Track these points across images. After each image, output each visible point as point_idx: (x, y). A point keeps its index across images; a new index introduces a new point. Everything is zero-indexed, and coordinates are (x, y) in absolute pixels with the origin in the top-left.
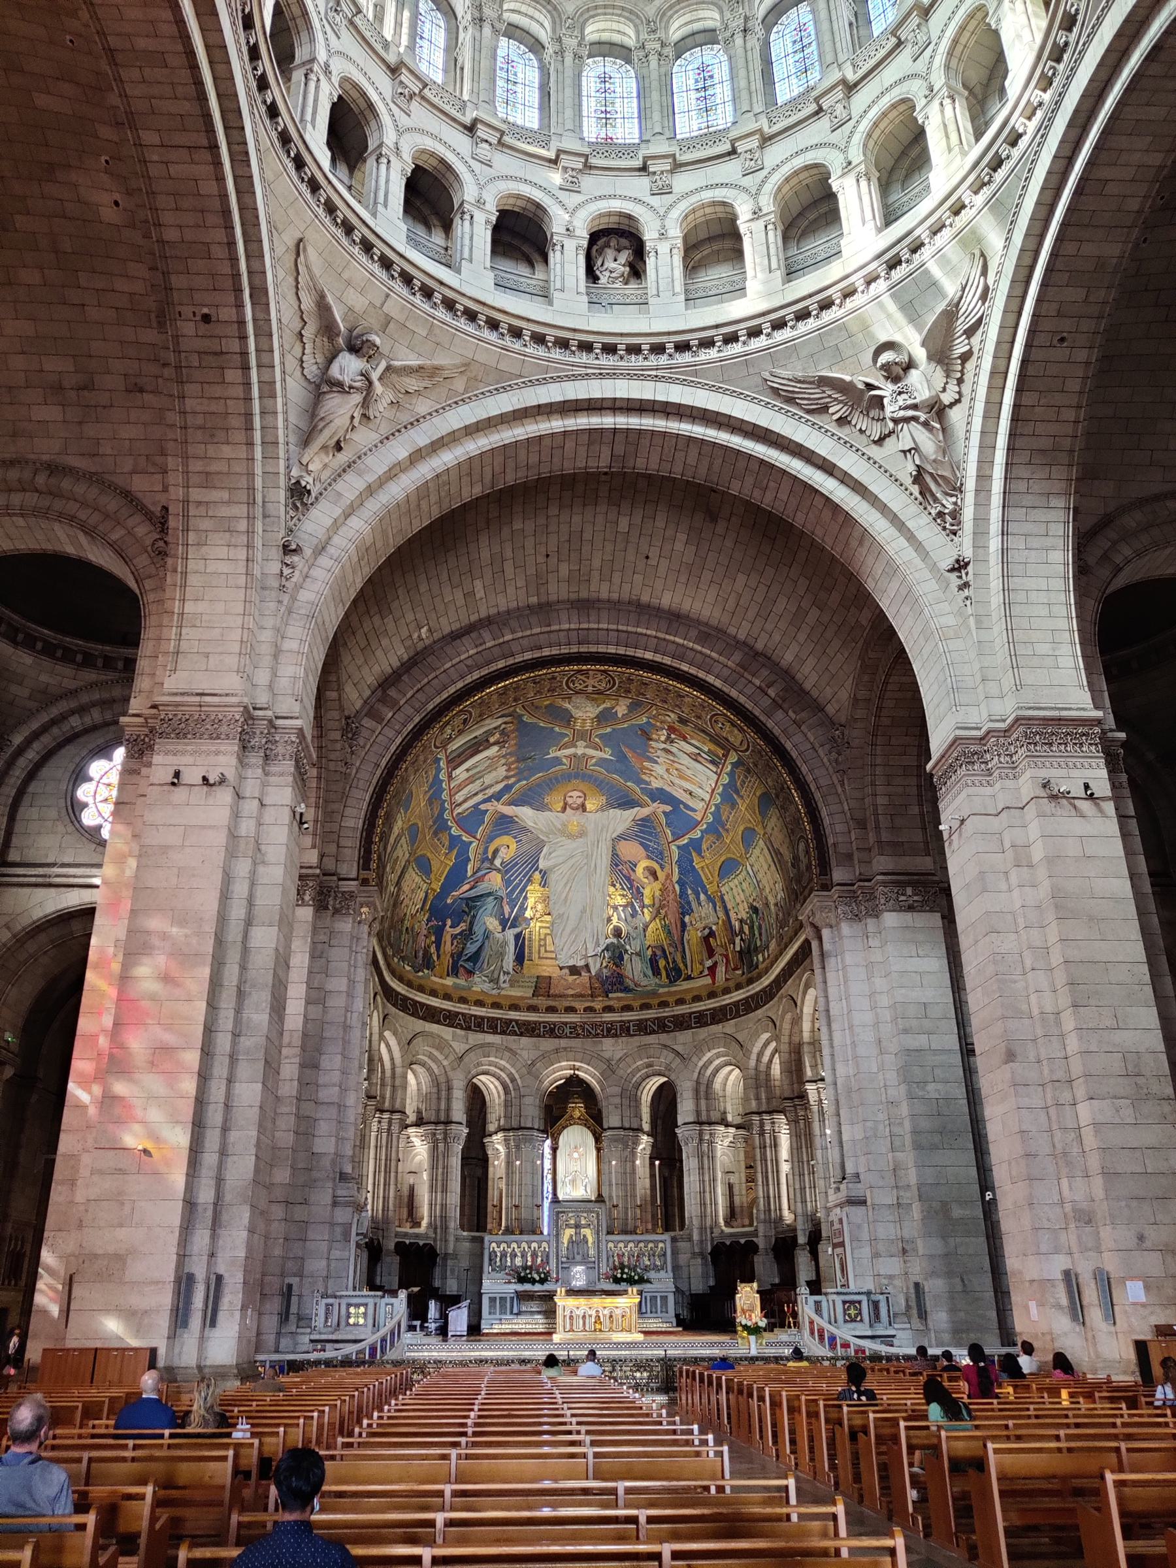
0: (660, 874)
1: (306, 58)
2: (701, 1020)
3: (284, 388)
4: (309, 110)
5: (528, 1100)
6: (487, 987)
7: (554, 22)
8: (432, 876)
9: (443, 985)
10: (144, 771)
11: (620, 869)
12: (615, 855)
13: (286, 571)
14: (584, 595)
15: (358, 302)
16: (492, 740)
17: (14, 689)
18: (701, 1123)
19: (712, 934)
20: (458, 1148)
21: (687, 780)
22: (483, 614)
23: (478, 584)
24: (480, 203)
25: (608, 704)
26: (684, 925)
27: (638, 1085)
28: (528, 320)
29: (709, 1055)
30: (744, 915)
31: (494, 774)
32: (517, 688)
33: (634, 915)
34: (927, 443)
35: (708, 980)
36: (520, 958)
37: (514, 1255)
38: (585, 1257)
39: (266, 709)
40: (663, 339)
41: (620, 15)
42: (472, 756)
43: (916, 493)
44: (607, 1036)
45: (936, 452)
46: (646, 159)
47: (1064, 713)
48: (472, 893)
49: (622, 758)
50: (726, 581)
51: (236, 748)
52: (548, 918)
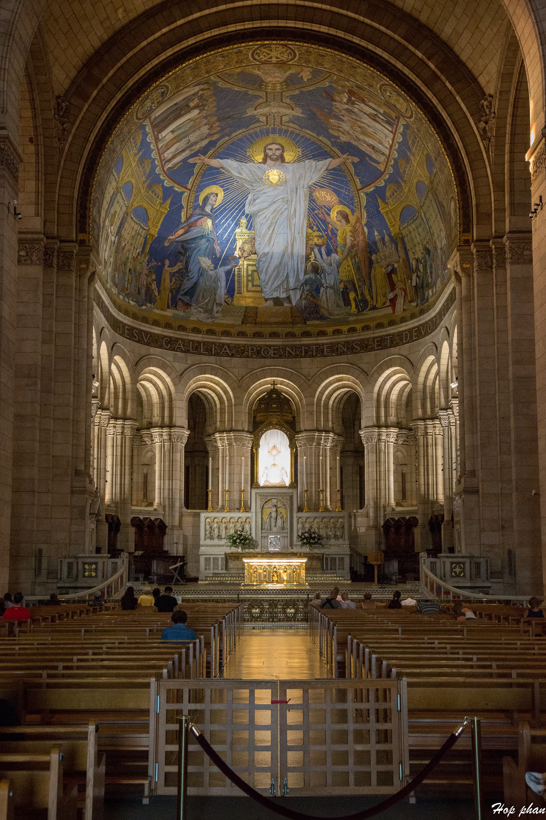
8: (150, 223)
9: (164, 316)
12: (312, 200)
16: (192, 105)
18: (379, 426)
19: (394, 271)
20: (181, 446)
21: (369, 137)
25: (293, 71)
26: (371, 263)
30: (419, 255)
31: (198, 133)
33: (329, 254)
35: (390, 310)
36: (231, 291)
44: (305, 357)
52: (254, 257)
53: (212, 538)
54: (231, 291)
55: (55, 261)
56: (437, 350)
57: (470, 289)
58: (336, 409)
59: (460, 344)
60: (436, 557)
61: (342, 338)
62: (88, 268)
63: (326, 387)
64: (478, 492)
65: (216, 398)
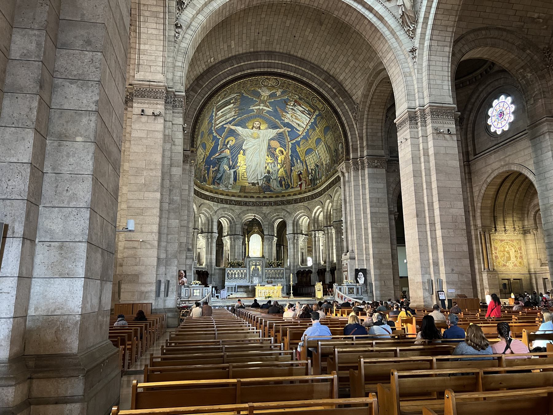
2: (296, 201)
5: (238, 226)
6: (224, 189)
11: (271, 151)
12: (269, 145)
13: (177, 35)
14: (270, 49)
16: (232, 102)
18: (294, 234)
19: (301, 173)
20: (215, 241)
22: (233, 54)
23: (233, 42)
26: (291, 170)
27: (274, 222)
29: (298, 212)
31: (230, 114)
32: (244, 83)
35: (299, 188)
36: (235, 179)
37: (235, 274)
38: (258, 274)
39: (172, 88)
43: (401, 22)
45: (410, 7)
47: (444, 105)
48: (219, 157)
49: (276, 111)
50: (322, 47)
51: (164, 103)
56: (322, 204)
60: (341, 285)
61: (279, 199)
64: (355, 259)
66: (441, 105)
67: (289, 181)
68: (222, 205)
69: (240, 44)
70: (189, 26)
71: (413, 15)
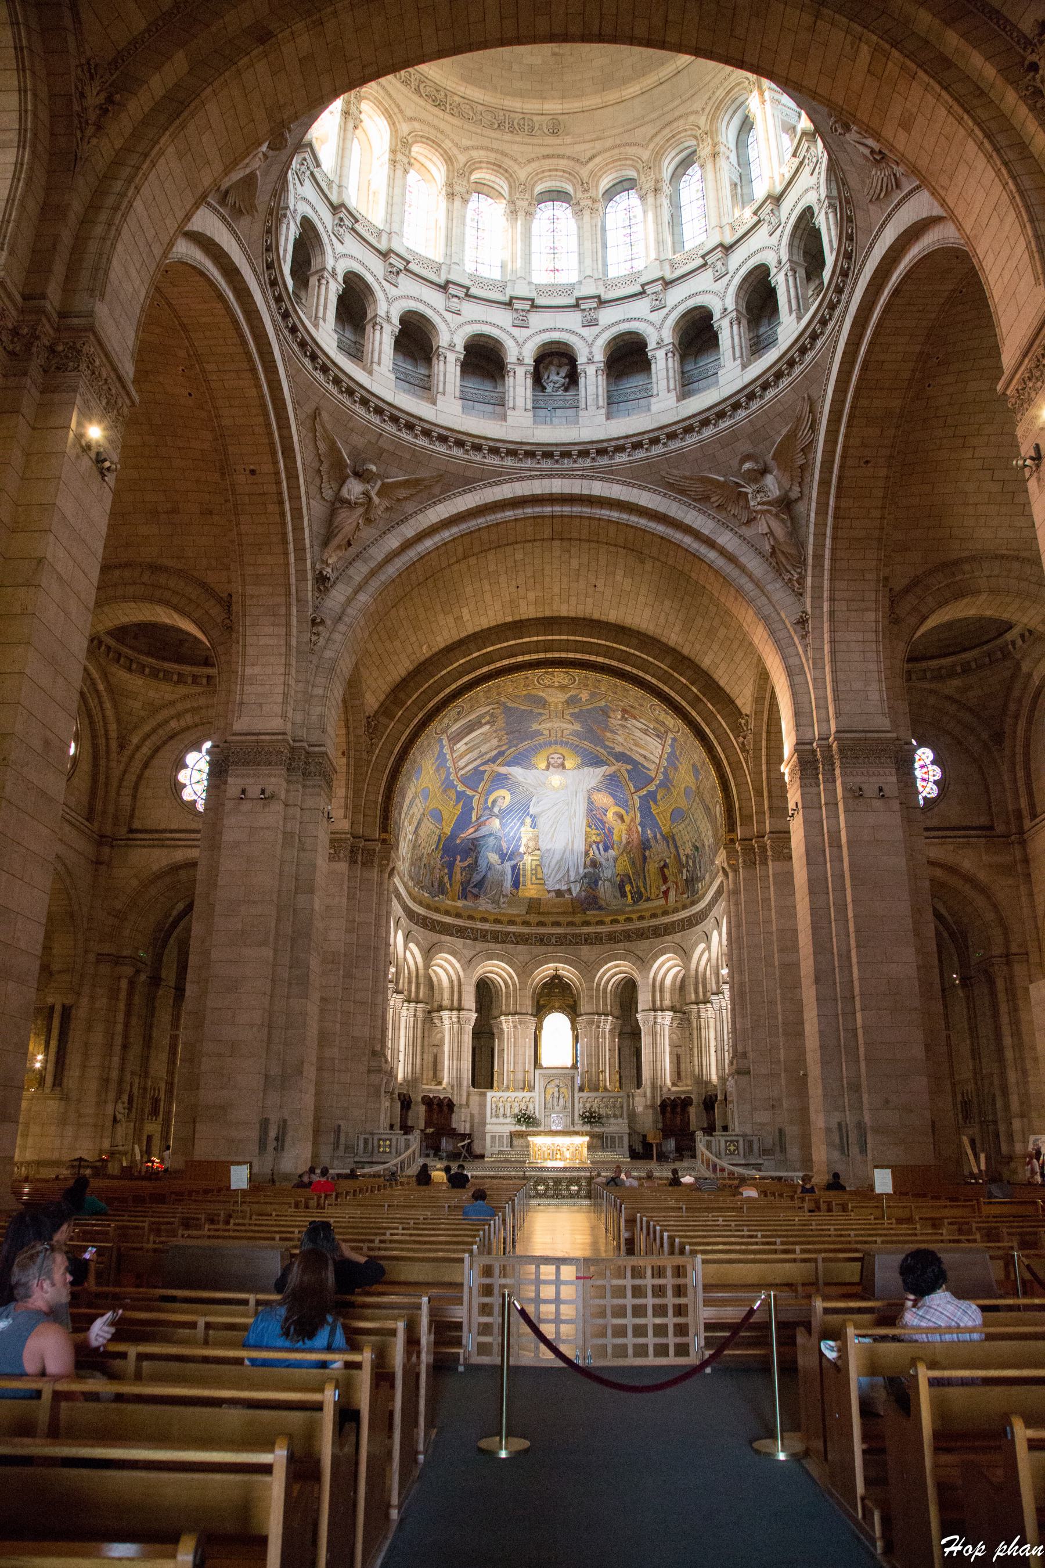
0: (625, 817)
1: (319, 267)
3: (309, 509)
4: (321, 308)
6: (490, 907)
7: (510, 187)
8: (444, 823)
9: (455, 907)
10: (223, 786)
12: (590, 802)
13: (314, 638)
14: (548, 613)
15: (359, 441)
16: (483, 721)
17: (131, 702)
18: (655, 1010)
19: (665, 866)
20: (469, 1028)
22: (470, 631)
23: (465, 611)
24: (452, 347)
25: (573, 693)
26: (645, 858)
28: (486, 438)
30: (689, 851)
31: (488, 744)
33: (606, 849)
34: (779, 531)
35: (662, 902)
36: (516, 884)
39: (302, 741)
40: (588, 447)
41: (562, 177)
42: (468, 734)
46: (578, 299)
53: (497, 1116)
54: (516, 884)
55: (360, 858)
56: (707, 937)
57: (736, 883)
58: (615, 994)
59: (729, 934)
60: (712, 1135)
61: (618, 927)
62: (388, 864)
63: (605, 973)
64: (749, 1072)
65: (502, 983)
66: (863, 735)
67: (641, 885)
68: (485, 945)
69: (482, 612)
70: (340, 618)
71: (792, 552)
